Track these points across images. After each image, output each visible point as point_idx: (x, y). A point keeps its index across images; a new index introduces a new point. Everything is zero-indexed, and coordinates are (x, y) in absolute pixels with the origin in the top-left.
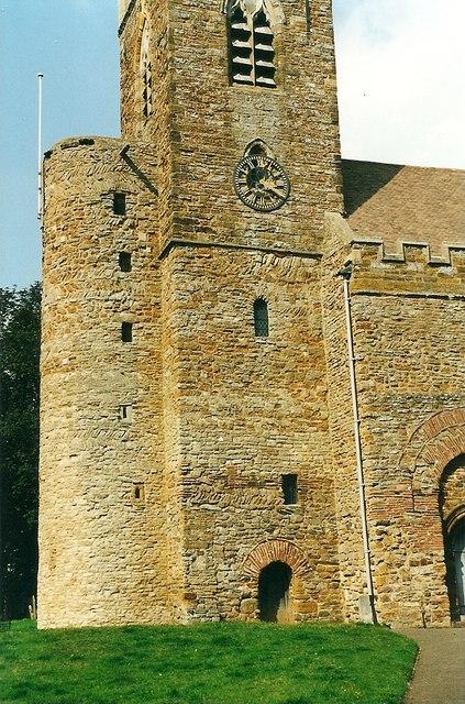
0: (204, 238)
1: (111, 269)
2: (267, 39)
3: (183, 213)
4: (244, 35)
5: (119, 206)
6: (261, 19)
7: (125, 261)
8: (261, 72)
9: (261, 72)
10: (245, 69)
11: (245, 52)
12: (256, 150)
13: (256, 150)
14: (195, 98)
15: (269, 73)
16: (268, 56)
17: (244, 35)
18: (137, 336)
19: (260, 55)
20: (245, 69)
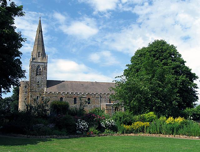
0: (33, 91)
1: (25, 93)
2: (41, 71)
3: (31, 89)
4: (38, 71)
5: (26, 88)
6: (40, 69)
7: (26, 92)
8: (40, 74)
9: (40, 74)
10: (38, 74)
11: (38, 73)
12: (38, 82)
13: (38, 82)
14: (33, 78)
15: (40, 74)
16: (41, 73)
17: (38, 71)
18: (27, 100)
19: (40, 73)
20: (38, 74)
